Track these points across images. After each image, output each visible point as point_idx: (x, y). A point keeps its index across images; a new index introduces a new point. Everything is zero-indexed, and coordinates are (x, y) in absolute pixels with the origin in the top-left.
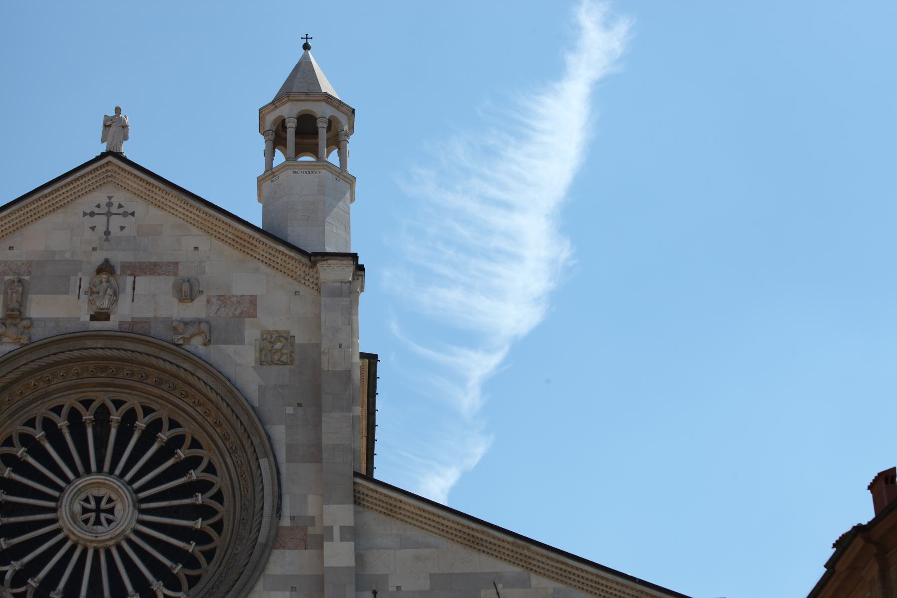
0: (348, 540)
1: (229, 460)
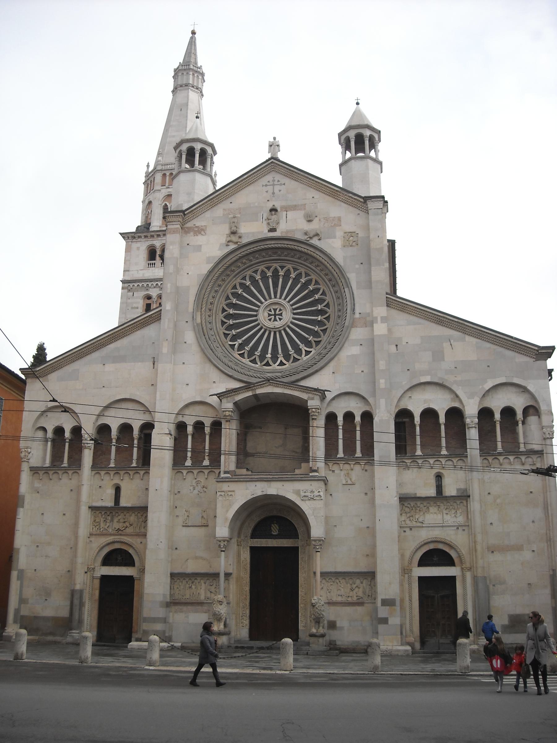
0: (384, 323)
1: (332, 290)
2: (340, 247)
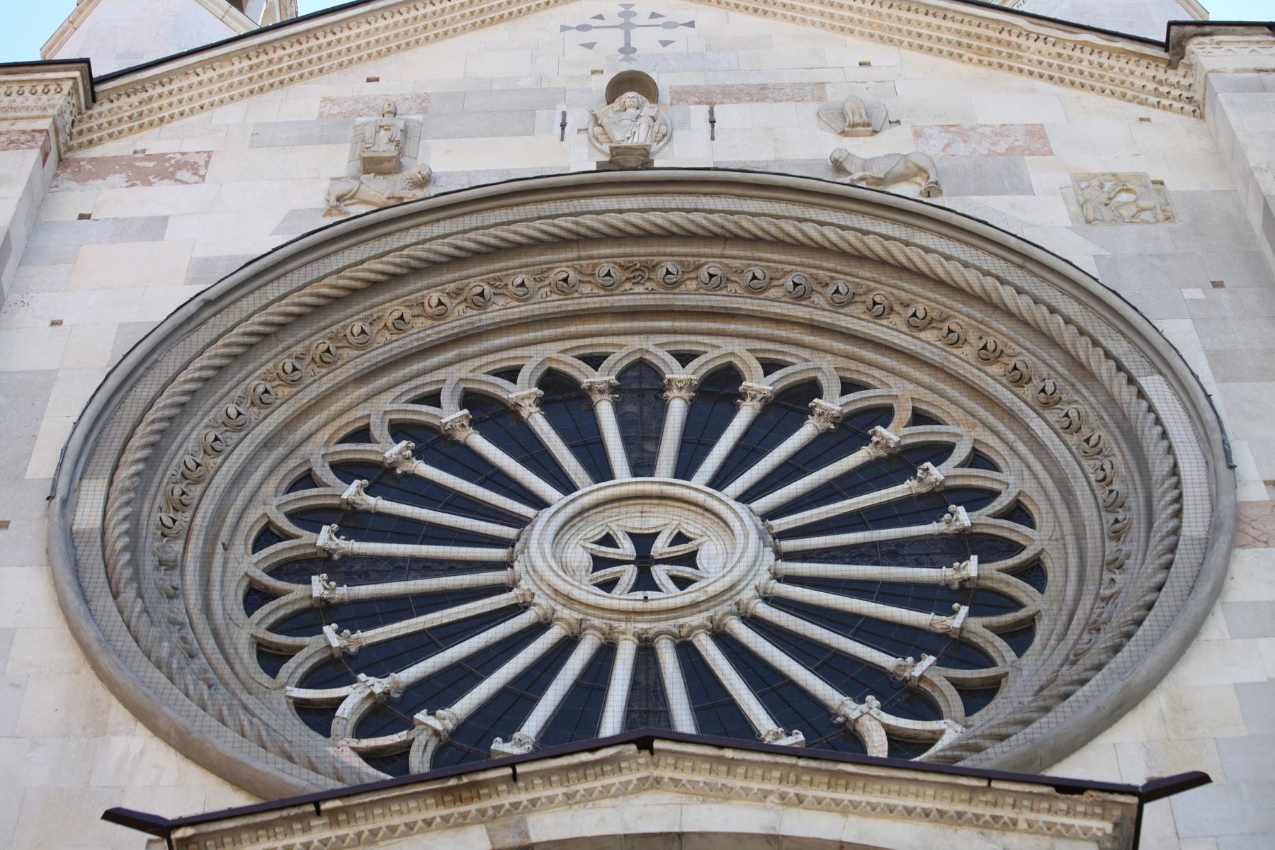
1: (1037, 425)
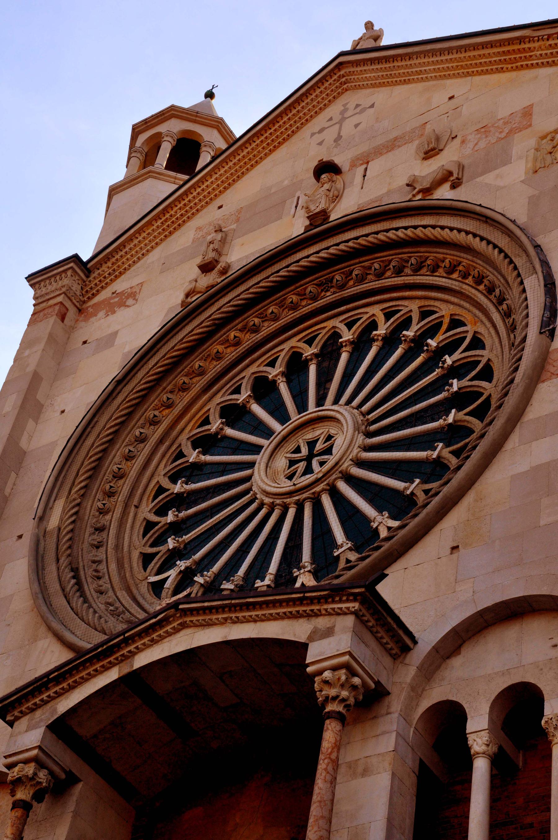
2: (523, 178)
